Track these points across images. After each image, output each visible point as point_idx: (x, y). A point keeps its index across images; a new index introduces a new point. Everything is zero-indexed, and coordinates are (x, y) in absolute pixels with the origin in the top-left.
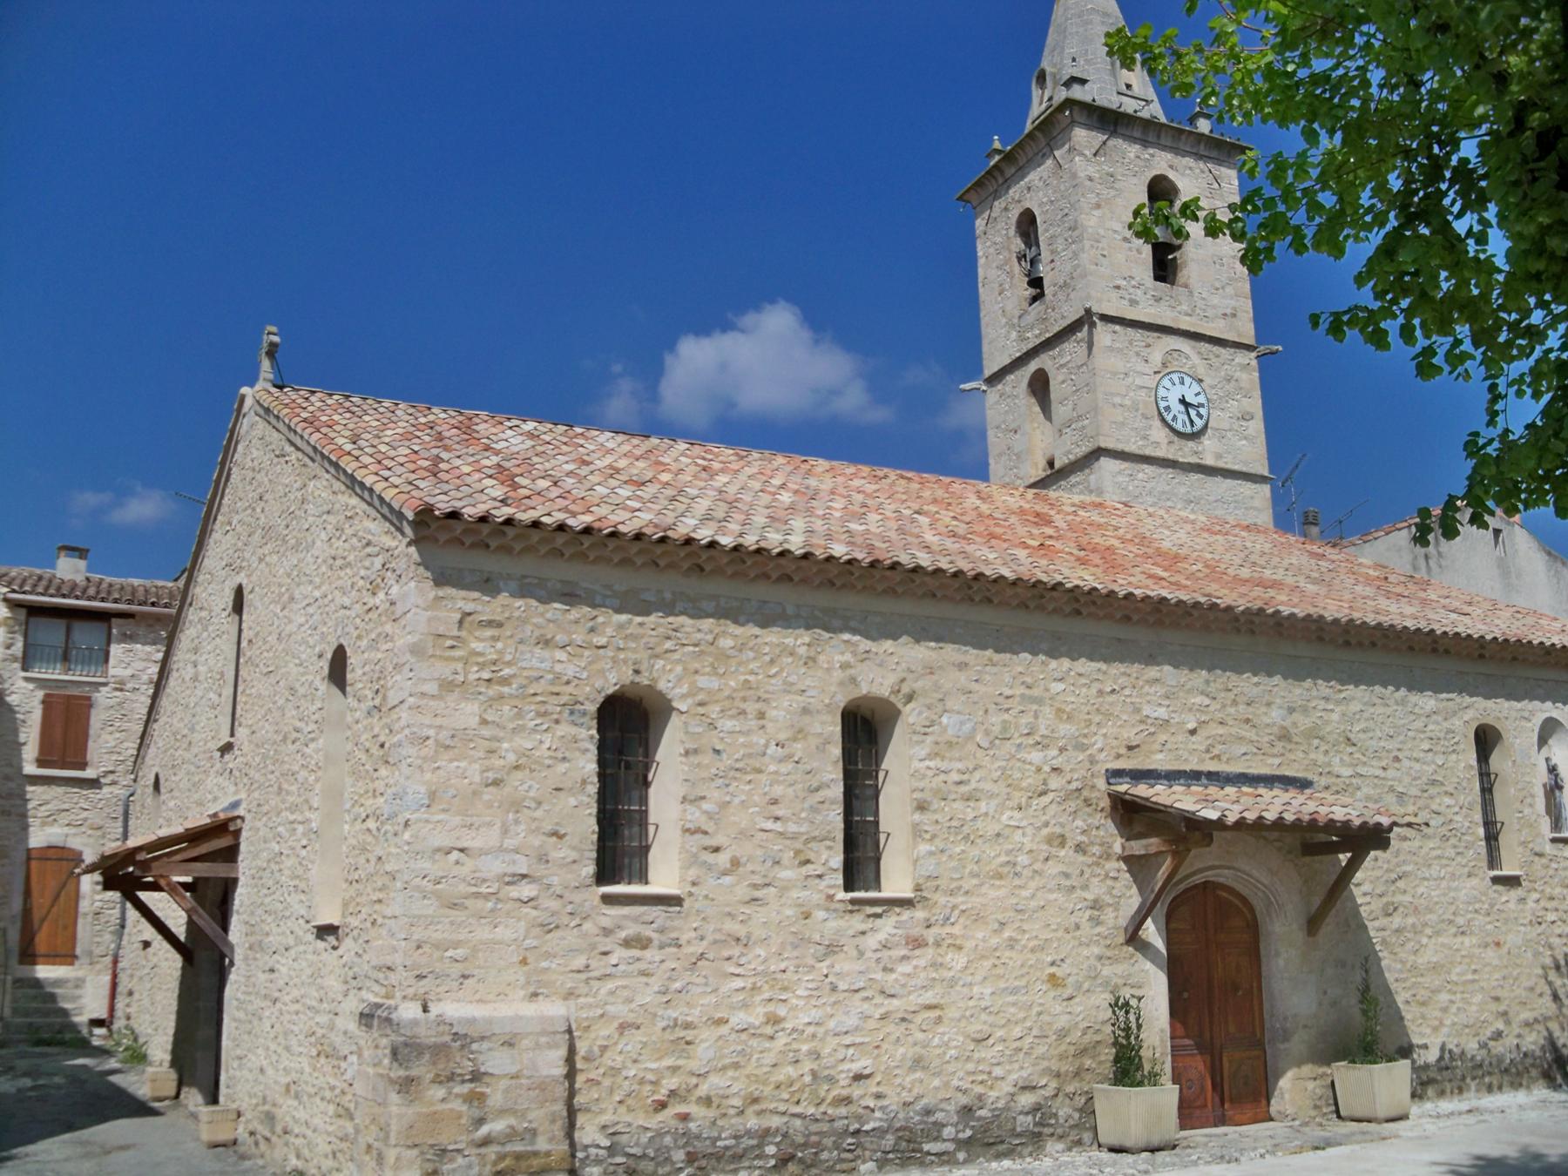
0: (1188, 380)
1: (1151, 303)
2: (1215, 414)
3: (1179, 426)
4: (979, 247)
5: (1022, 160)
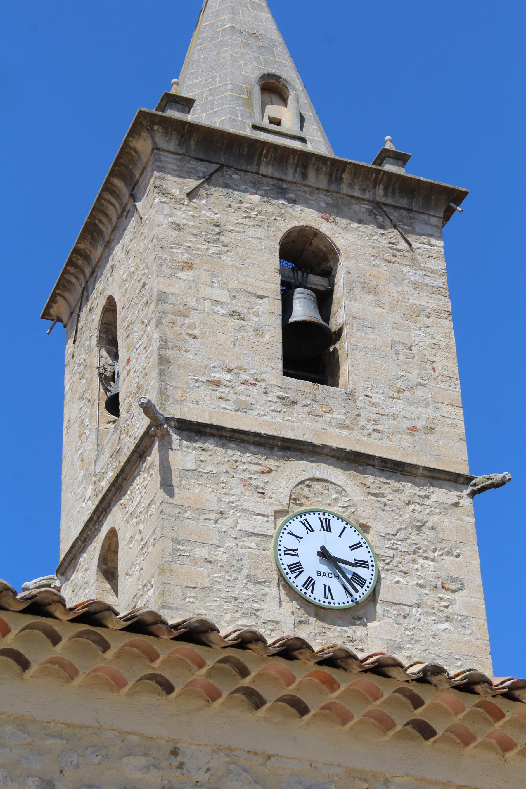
0: (336, 525)
1: (274, 403)
2: (388, 579)
3: (317, 595)
4: (67, 377)
5: (107, 230)
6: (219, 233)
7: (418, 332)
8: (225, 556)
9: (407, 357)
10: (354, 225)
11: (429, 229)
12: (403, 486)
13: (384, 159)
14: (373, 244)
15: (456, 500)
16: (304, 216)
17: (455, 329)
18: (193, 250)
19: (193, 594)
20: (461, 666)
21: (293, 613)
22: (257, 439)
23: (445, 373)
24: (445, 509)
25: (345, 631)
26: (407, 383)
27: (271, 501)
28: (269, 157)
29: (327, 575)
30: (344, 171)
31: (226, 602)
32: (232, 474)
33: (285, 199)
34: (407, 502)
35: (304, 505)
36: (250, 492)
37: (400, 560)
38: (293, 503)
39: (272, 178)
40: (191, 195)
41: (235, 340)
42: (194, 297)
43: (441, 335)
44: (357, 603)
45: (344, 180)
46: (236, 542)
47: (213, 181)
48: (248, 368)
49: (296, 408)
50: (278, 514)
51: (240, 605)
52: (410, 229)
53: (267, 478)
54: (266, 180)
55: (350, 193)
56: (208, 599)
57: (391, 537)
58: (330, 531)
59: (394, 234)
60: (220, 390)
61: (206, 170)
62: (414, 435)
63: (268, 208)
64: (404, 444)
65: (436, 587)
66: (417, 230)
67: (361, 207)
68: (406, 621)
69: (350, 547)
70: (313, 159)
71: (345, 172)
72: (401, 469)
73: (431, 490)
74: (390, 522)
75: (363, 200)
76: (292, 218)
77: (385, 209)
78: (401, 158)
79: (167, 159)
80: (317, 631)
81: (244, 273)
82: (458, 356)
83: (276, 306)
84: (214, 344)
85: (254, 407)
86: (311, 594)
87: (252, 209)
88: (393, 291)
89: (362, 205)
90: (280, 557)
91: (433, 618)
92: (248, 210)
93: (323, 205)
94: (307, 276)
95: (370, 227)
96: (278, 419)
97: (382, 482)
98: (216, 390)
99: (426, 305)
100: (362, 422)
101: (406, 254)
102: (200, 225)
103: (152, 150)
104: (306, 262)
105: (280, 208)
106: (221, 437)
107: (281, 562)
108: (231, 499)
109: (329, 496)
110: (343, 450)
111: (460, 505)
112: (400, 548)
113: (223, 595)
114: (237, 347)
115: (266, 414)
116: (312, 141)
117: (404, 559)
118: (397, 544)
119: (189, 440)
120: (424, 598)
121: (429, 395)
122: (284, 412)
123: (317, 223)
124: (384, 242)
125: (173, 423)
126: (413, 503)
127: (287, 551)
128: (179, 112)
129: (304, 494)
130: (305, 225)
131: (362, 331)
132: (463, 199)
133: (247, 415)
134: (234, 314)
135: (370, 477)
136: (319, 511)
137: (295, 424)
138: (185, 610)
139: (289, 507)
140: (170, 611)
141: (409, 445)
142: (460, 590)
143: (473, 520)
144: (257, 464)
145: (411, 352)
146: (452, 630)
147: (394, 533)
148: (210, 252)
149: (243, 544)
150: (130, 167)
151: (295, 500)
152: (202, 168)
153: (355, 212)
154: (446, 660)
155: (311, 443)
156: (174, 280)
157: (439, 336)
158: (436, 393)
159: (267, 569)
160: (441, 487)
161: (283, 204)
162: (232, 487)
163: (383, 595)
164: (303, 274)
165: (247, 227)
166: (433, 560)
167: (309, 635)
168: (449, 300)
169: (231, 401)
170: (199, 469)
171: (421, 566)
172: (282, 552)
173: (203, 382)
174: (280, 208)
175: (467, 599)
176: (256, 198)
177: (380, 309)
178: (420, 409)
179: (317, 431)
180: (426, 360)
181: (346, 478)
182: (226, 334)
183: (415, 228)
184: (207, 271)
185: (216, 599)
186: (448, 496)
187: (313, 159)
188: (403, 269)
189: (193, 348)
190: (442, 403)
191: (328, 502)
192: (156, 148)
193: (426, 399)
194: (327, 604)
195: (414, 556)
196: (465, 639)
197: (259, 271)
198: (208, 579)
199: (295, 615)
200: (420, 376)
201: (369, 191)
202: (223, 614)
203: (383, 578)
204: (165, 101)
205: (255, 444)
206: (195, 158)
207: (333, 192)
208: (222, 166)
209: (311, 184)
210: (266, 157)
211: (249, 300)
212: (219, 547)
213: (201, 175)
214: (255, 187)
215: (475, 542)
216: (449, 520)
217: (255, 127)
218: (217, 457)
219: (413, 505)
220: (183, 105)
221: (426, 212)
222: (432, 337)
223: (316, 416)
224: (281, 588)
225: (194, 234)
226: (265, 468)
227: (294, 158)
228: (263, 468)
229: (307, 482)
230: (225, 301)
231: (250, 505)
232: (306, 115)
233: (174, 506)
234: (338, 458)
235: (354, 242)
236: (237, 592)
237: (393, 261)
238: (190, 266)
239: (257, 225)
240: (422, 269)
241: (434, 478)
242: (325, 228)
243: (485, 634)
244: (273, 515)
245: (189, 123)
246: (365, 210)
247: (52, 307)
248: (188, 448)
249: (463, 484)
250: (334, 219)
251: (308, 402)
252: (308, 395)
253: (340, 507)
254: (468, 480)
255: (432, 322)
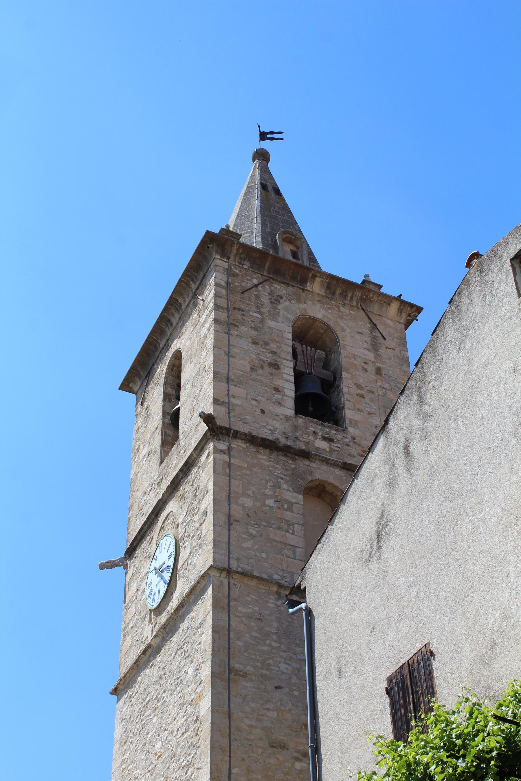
210: (158, 339)
227: (162, 324)
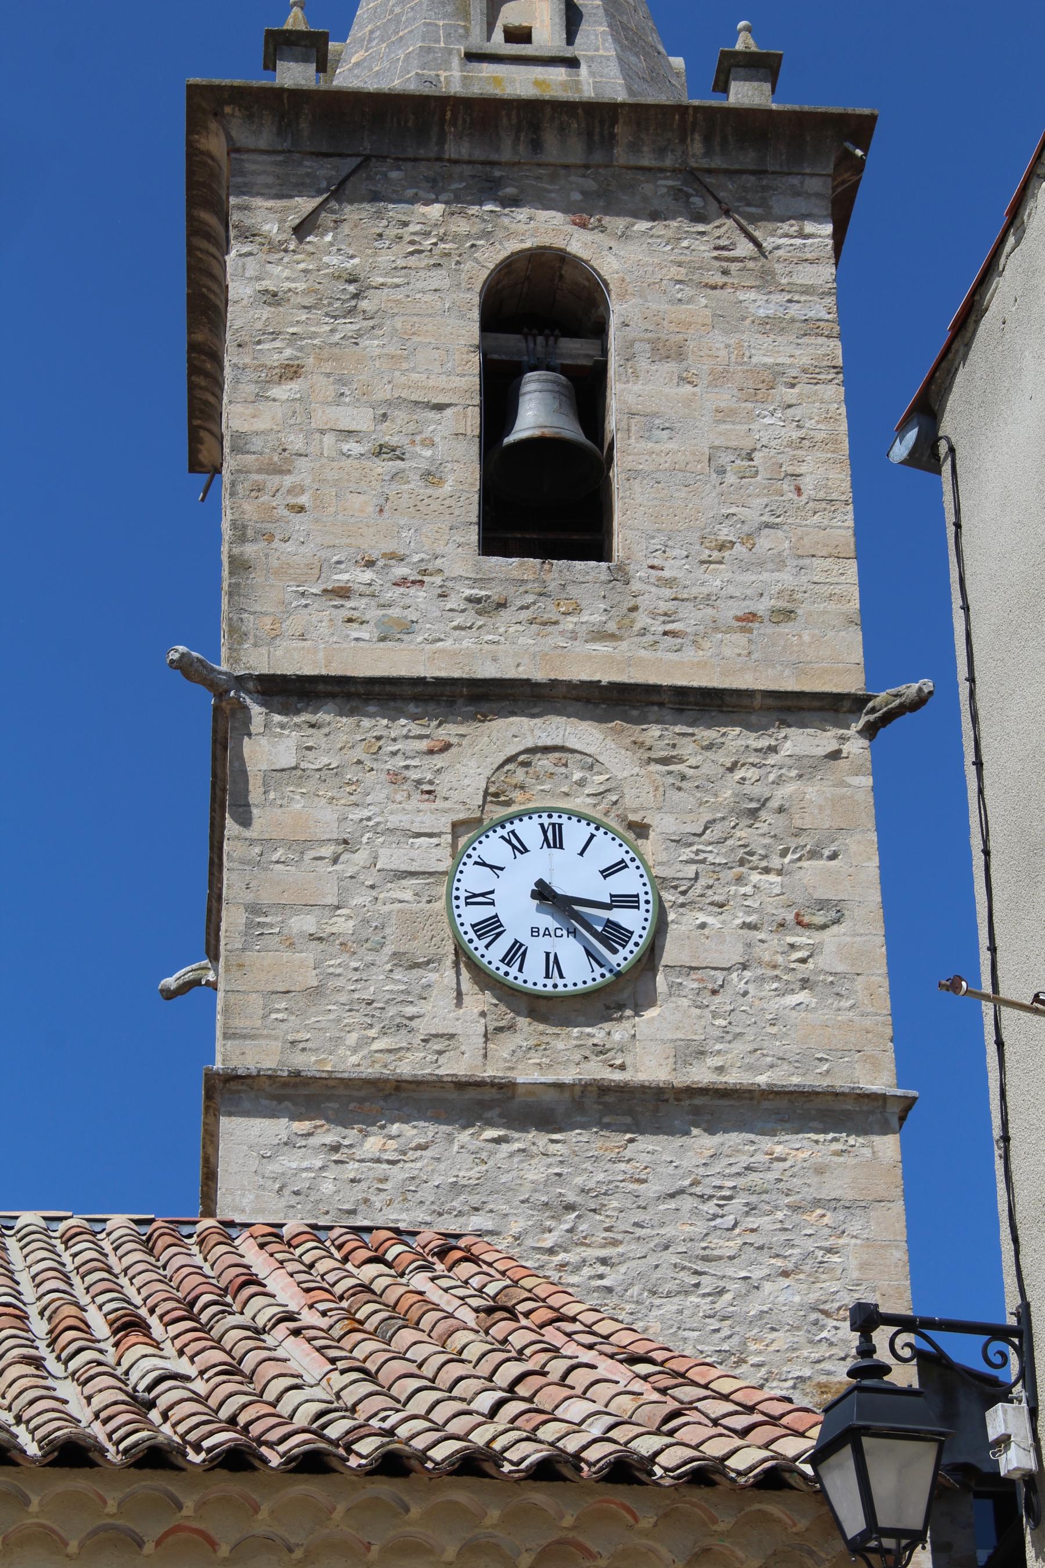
0: (575, 833)
2: (682, 925)
3: (532, 975)
6: (356, 296)
7: (767, 421)
8: (351, 923)
9: (740, 475)
10: (642, 225)
11: (801, 205)
12: (724, 735)
13: (729, 71)
14: (682, 258)
15: (834, 746)
16: (538, 228)
17: (848, 400)
18: (302, 339)
19: (283, 1005)
20: (828, 1071)
21: (483, 1014)
22: (420, 689)
23: (821, 495)
24: (808, 768)
25: (589, 1035)
26: (740, 528)
27: (447, 805)
28: (460, 122)
29: (552, 934)
30: (614, 122)
31: (350, 1010)
32: (369, 764)
33: (495, 200)
34: (729, 765)
35: (514, 802)
36: (405, 794)
37: (711, 882)
38: (491, 802)
39: (469, 162)
40: (301, 230)
41: (382, 501)
42: (302, 430)
43: (817, 418)
44: (618, 975)
45: (619, 138)
46: (374, 893)
47: (347, 192)
48: (407, 553)
49: (505, 614)
50: (458, 828)
51: (377, 1013)
52: (760, 211)
53: (438, 761)
54: (457, 169)
55: (633, 161)
56: (313, 1009)
57: (692, 839)
58: (561, 847)
59: (725, 228)
60: (349, 604)
61: (334, 173)
62: (750, 631)
63: (461, 226)
64: (727, 652)
65: (782, 925)
66: (776, 210)
67: (658, 186)
68: (717, 999)
69: (602, 872)
70: (548, 111)
71: (617, 122)
72: (719, 702)
73: (783, 735)
74: (691, 811)
75: (661, 170)
76: (508, 237)
77: (708, 180)
78: (763, 66)
79: (254, 167)
80: (532, 1042)
81: (405, 366)
82: (851, 456)
83: (469, 419)
84: (340, 517)
85: (416, 626)
86: (518, 974)
87: (427, 234)
88: (717, 345)
89: (660, 182)
90: (456, 912)
91: (775, 985)
92: (417, 238)
93: (577, 196)
94: (556, 342)
95: (674, 224)
96: (465, 644)
97: (679, 734)
98: (342, 606)
99: (788, 361)
100: (642, 620)
101: (751, 264)
102: (318, 286)
103: (228, 154)
104: (541, 318)
105: (484, 221)
106: (349, 696)
107: (458, 921)
108: (366, 813)
109: (567, 777)
110: (595, 685)
111: (844, 755)
112: (711, 858)
113: (343, 998)
114: (386, 515)
115: (442, 636)
116: (591, 59)
117: (718, 879)
118: (704, 852)
119: (284, 711)
120: (758, 950)
121: (787, 544)
122: (480, 627)
123: (562, 237)
124: (704, 249)
125: (251, 685)
126: (743, 765)
127: (472, 899)
128: (297, 61)
129: (514, 782)
130: (535, 245)
131: (649, 438)
132: (872, 129)
133: (403, 645)
134: (381, 451)
135: (654, 727)
136: (539, 811)
137: (500, 647)
138: (267, 1037)
139: (482, 811)
140: (237, 1042)
141: (737, 651)
142: (834, 923)
143: (868, 781)
144: (421, 737)
145: (751, 463)
146: (813, 1005)
147: (700, 830)
148: (337, 337)
149: (388, 895)
150: (214, 186)
151: (496, 795)
152: (326, 170)
153: (645, 199)
154: (796, 1065)
155: (528, 680)
156: (262, 406)
157: (813, 421)
158: (802, 538)
159: (433, 937)
160: (803, 725)
161: (492, 211)
162: (369, 790)
163: (671, 953)
164: (547, 341)
165: (413, 273)
166: (780, 872)
167: (514, 1051)
168: (839, 344)
169: (372, 623)
170: (303, 765)
171: (755, 886)
172: (461, 902)
173: (316, 595)
174: (484, 221)
175: (848, 939)
176: (436, 210)
177: (689, 387)
178: (765, 576)
179: (547, 654)
180: (783, 474)
181: (602, 737)
182: (365, 493)
183: (771, 208)
184: (328, 375)
185: (329, 1007)
186: (816, 742)
187: (548, 111)
188: (741, 298)
189: (298, 531)
190: (813, 556)
191: (565, 789)
192: (234, 149)
193: (780, 554)
194: (550, 988)
195: (741, 869)
196: (840, 1018)
197: (437, 356)
198: (314, 972)
199: (489, 1017)
200: (768, 509)
201: (672, 151)
202: (343, 1034)
203: (672, 921)
204: (271, 47)
205: (416, 699)
206: (312, 153)
207: (598, 166)
208: (367, 158)
209: (551, 160)
210: (454, 124)
211: (415, 417)
212: (338, 908)
213: (324, 184)
214: (435, 189)
215: (871, 824)
216: (816, 788)
217: (472, 57)
218: (341, 734)
219: (743, 769)
220: (306, 46)
221: (795, 170)
222: (798, 426)
223: (545, 624)
224: (464, 970)
225: (305, 307)
226: (437, 743)
228: (433, 743)
229: (521, 758)
230: (364, 429)
231: (404, 818)
232: (586, 6)
233: (252, 842)
234: (588, 701)
235: (636, 262)
236: (372, 989)
237: (720, 284)
238: (296, 372)
239: (434, 265)
240: (782, 290)
241: (789, 709)
242: (578, 243)
243: (884, 1004)
244: (449, 831)
245: (288, 90)
246: (665, 190)
247: (199, 451)
248: (282, 726)
249: (851, 711)
250: (600, 221)
251: (530, 599)
252: (530, 586)
253: (588, 795)
254: (857, 703)
255: (800, 394)
